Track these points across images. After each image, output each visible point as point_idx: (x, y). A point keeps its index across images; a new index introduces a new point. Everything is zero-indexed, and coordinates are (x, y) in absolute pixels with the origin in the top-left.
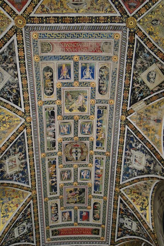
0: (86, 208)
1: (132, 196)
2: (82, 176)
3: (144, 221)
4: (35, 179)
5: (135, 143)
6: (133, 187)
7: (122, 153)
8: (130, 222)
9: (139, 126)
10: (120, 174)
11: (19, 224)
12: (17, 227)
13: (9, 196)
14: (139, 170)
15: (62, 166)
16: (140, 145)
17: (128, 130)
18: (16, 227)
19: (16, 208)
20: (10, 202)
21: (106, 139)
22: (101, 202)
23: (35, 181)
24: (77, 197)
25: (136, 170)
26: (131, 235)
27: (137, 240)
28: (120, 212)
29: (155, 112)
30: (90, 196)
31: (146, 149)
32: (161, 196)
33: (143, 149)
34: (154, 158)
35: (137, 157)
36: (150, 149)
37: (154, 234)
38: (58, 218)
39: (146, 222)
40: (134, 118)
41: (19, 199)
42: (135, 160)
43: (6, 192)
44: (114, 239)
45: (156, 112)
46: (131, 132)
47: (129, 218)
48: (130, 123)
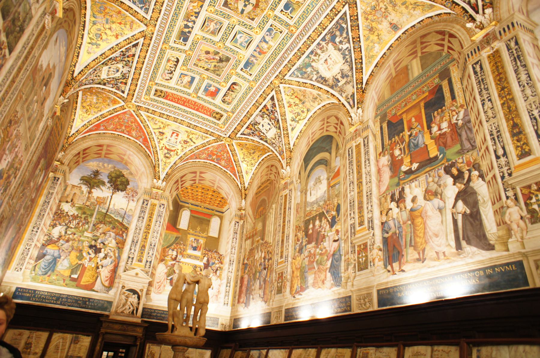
0: (219, 83)
1: (291, 100)
2: (237, 40)
3: (288, 134)
4: (161, 10)
5: (341, 39)
6: (300, 91)
7: (315, 40)
8: (269, 126)
9: (365, 17)
10: (293, 66)
11: (113, 63)
12: (108, 67)
13: (108, 17)
14: (323, 76)
15: (213, 11)
16: (347, 45)
17: (345, 13)
18: (107, 65)
19: (114, 38)
20: (107, 26)
21: (305, 7)
22: (244, 85)
23: (160, 13)
24: (213, 64)
25: (318, 73)
26: (261, 139)
27: (266, 148)
28: (263, 108)
30: (234, 72)
31: (351, 57)
32: (328, 120)
33: (347, 53)
34: (353, 74)
35: (331, 59)
36: (356, 60)
37: (291, 152)
38: (171, 78)
39: (290, 136)
40: (366, 2)
41: (123, 28)
42: (326, 60)
43: (106, 8)
44: (237, 134)
45: (402, 13)
48: (355, 5)
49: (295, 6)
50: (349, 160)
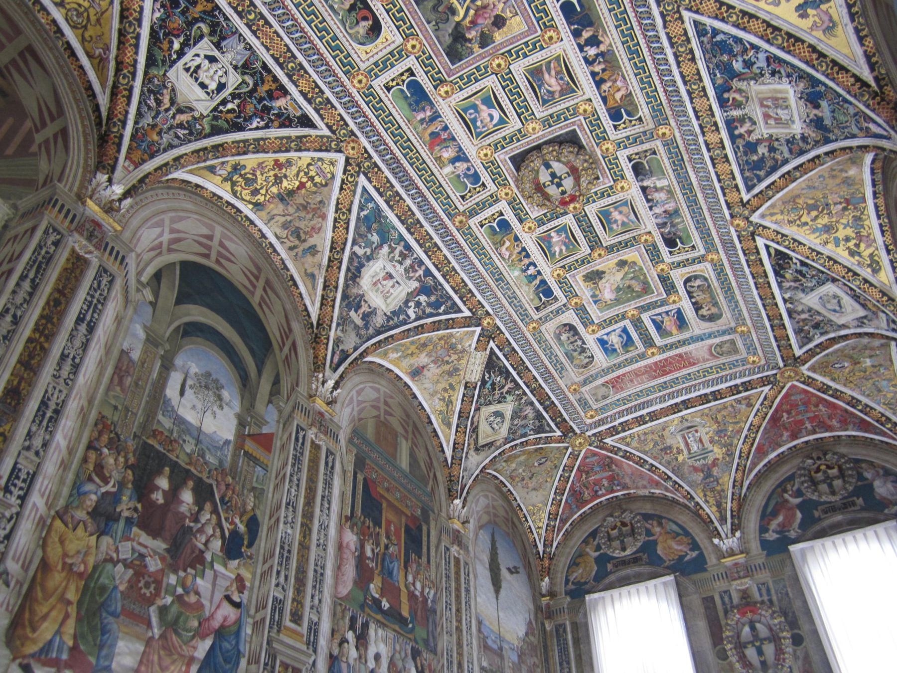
5: (424, 304)
7: (429, 257)
8: (213, 86)
10: (387, 202)
14: (363, 270)
16: (413, 316)
17: (460, 311)
25: (369, 258)
28: (275, 79)
29: (438, 382)
31: (396, 326)
33: (401, 318)
35: (393, 287)
36: (392, 336)
42: (390, 276)
46: (450, 313)
47: (234, 96)
49: (498, 238)
50: (295, 449)
